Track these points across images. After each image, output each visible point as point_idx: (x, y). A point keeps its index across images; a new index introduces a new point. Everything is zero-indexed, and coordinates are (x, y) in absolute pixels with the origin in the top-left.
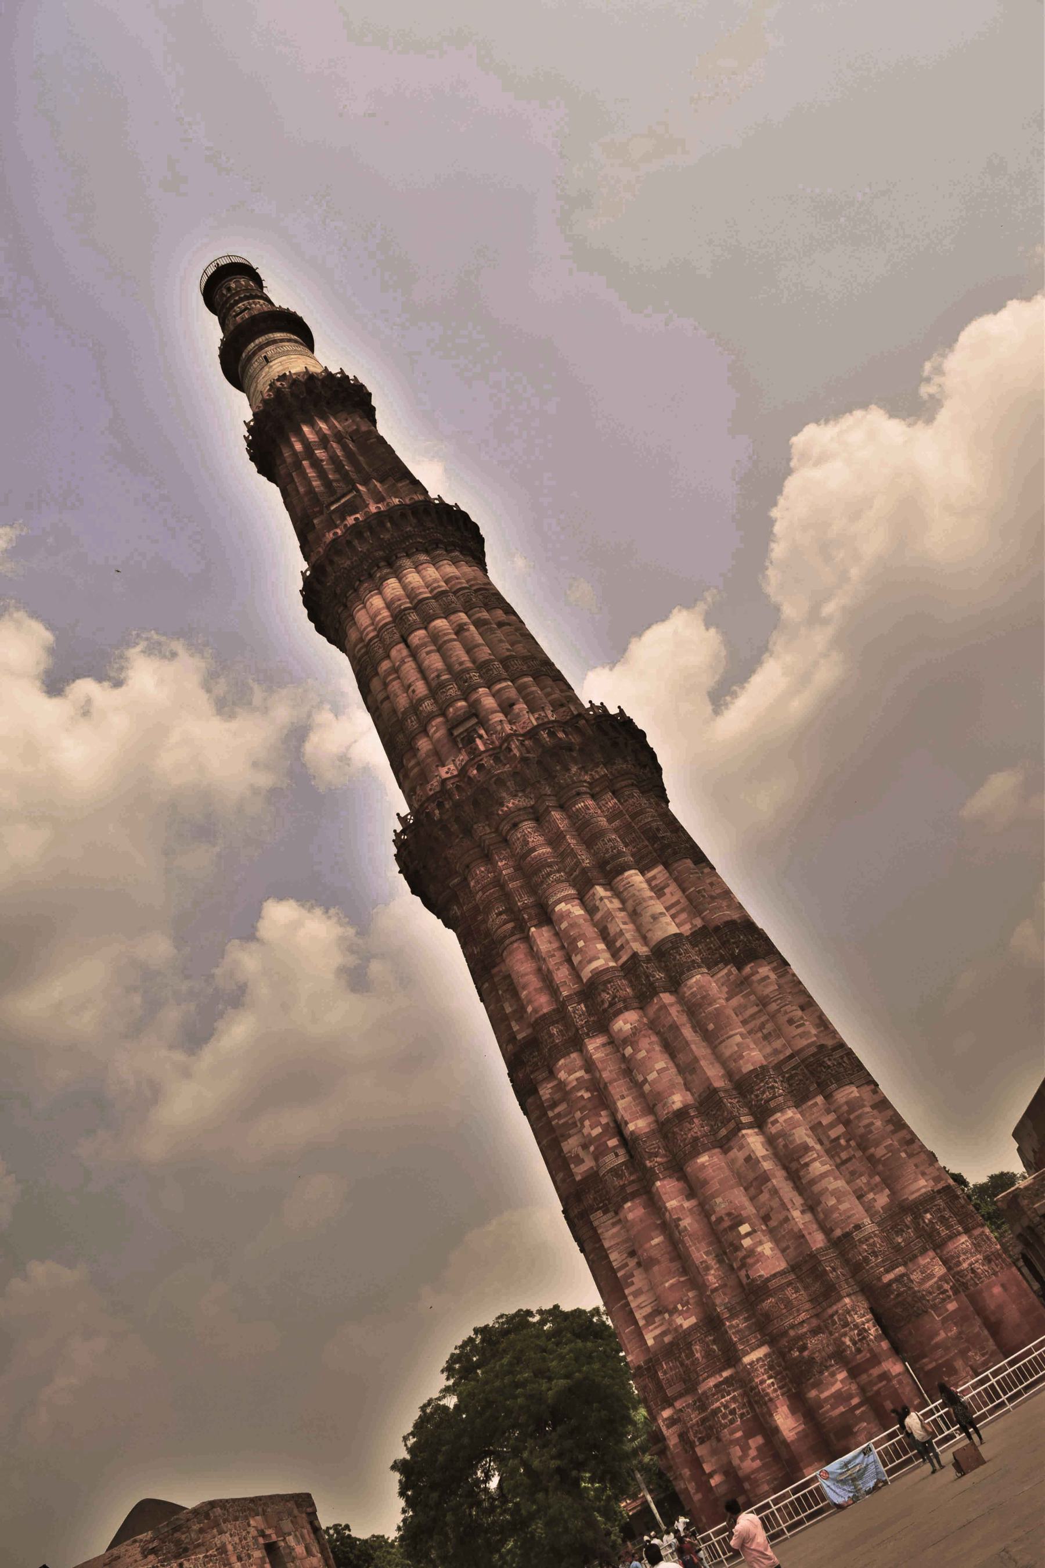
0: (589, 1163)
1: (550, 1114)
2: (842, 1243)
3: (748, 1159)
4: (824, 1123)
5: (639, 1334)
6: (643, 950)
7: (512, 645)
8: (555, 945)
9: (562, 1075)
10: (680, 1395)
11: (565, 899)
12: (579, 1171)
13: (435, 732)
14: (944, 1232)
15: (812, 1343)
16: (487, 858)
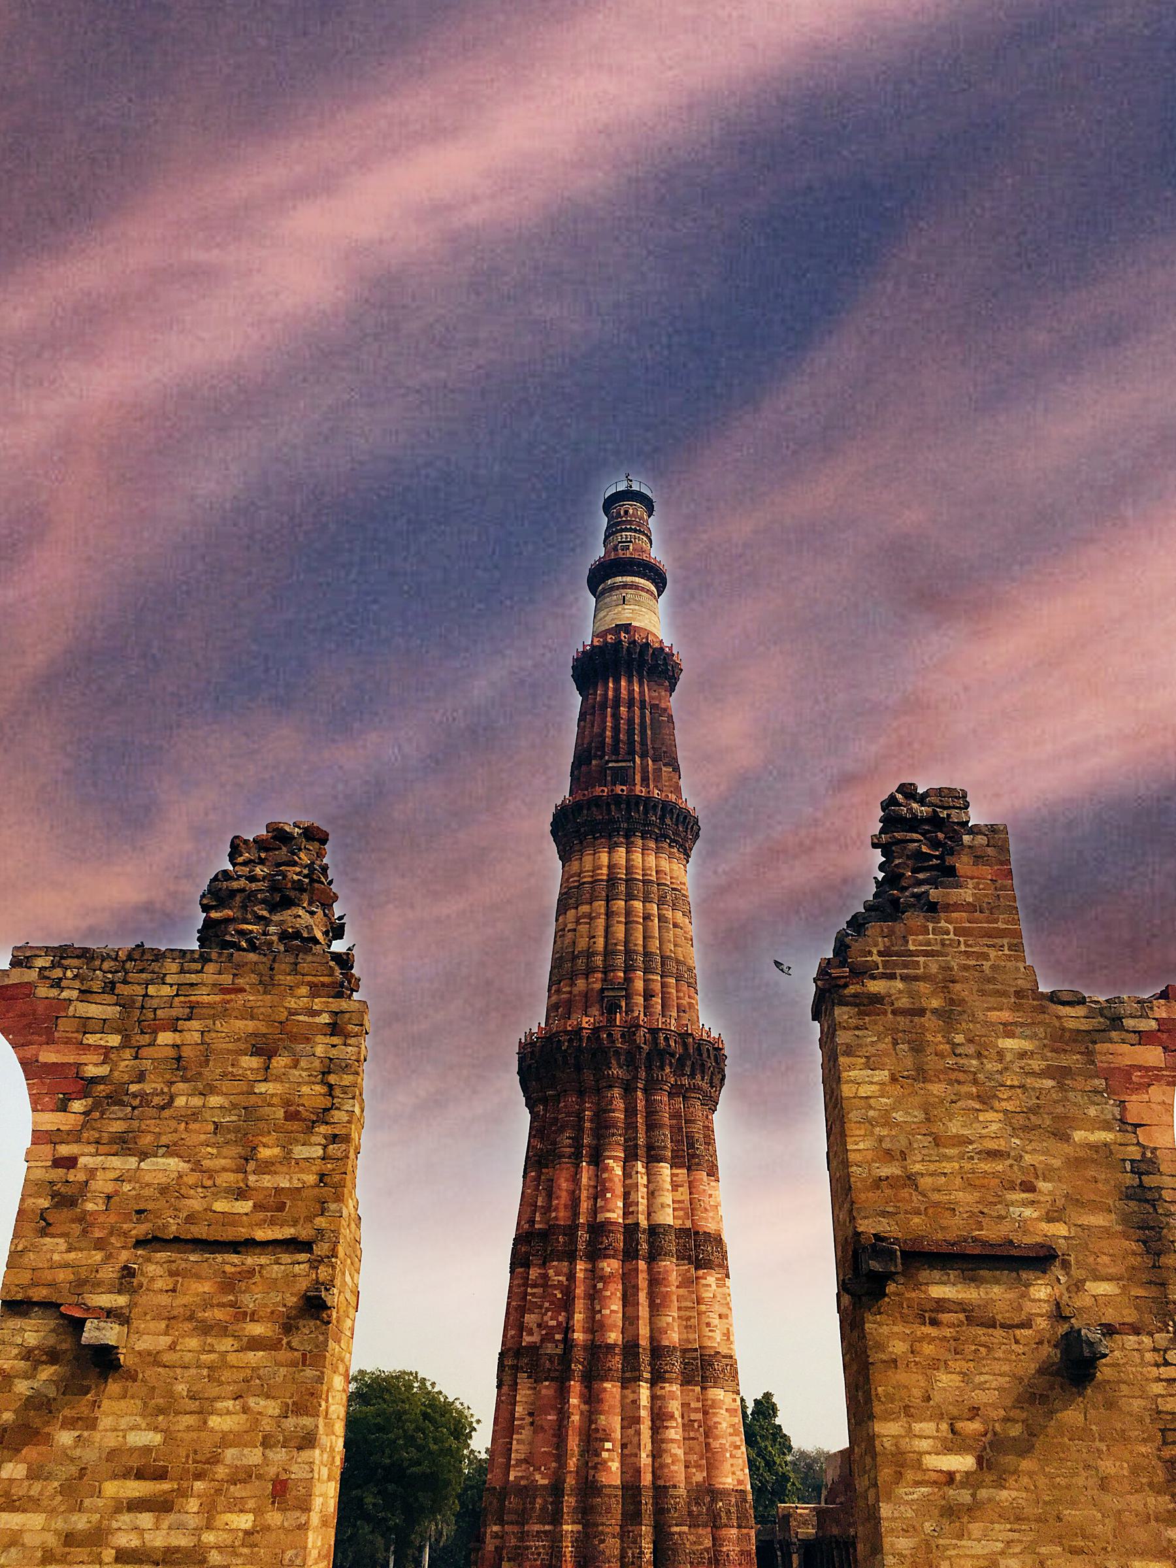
0: (535, 1338)
1: (529, 1290)
2: (661, 1491)
3: (634, 1402)
4: (692, 1405)
5: (507, 1467)
6: (644, 1223)
7: (675, 945)
8: (592, 1183)
9: (551, 1272)
10: (512, 1523)
11: (615, 1158)
12: (527, 1339)
13: (594, 983)
14: (724, 1520)
15: (610, 1541)
16: (581, 1093)
